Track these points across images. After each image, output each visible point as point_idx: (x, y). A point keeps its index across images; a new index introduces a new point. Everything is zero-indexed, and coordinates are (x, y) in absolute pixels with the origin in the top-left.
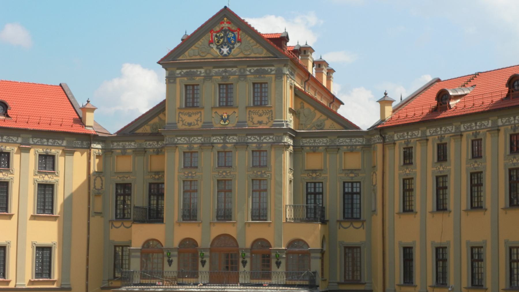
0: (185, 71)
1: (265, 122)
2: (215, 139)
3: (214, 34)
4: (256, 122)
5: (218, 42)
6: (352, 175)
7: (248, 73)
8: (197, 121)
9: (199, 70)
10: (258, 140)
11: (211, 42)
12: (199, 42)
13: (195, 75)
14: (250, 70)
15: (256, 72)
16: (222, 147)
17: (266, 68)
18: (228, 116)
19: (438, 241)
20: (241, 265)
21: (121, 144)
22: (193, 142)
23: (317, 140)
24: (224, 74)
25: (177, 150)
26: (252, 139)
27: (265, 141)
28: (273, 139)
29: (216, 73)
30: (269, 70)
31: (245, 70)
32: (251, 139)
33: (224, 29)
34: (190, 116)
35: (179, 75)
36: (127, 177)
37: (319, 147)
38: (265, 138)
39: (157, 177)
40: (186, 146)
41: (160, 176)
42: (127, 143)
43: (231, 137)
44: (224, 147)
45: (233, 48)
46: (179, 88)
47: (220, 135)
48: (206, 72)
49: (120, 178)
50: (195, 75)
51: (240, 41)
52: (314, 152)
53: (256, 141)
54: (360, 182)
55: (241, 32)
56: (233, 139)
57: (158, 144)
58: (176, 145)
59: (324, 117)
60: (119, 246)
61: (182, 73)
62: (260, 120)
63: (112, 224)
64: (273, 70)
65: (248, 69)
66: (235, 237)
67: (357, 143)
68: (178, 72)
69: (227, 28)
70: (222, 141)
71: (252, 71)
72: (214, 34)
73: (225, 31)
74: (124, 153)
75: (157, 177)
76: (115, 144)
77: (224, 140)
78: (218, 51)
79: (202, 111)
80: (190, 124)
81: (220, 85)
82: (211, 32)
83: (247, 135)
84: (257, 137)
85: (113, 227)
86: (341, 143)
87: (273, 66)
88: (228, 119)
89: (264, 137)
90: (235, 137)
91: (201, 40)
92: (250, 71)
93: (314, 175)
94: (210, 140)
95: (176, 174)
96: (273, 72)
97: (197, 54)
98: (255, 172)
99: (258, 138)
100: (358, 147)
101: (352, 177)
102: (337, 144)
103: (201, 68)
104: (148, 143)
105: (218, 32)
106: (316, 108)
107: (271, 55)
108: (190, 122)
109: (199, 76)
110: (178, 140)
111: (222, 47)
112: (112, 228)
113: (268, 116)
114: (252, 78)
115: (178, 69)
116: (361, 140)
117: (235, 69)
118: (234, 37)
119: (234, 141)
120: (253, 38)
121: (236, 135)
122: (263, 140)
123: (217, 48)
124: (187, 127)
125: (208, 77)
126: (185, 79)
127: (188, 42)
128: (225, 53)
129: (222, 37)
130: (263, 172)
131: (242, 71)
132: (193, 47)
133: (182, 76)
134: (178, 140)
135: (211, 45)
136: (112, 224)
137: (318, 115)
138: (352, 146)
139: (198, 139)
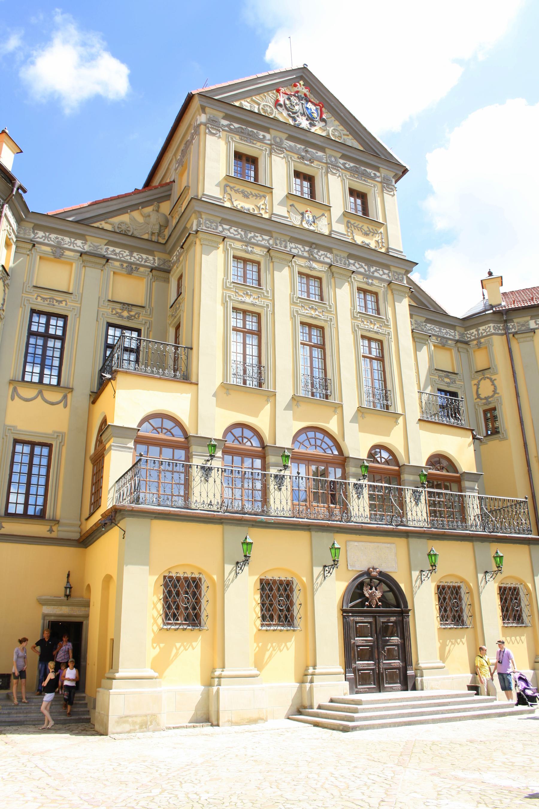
0: (237, 125)
9: (262, 133)
10: (365, 271)
14: (345, 164)
17: (369, 170)
21: (53, 236)
22: (253, 240)
24: (303, 154)
27: (376, 274)
28: (389, 277)
35: (226, 128)
36: (61, 302)
39: (125, 314)
41: (132, 313)
42: (67, 239)
43: (322, 252)
49: (44, 299)
53: (362, 270)
57: (131, 255)
60: (24, 443)
63: (15, 389)
64: (378, 177)
67: (448, 336)
68: (225, 122)
71: (347, 166)
74: (58, 253)
75: (125, 314)
76: (41, 234)
77: (310, 253)
84: (363, 264)
85: (16, 397)
86: (429, 330)
87: (377, 169)
89: (374, 268)
90: (329, 255)
92: (344, 164)
96: (379, 179)
99: (366, 268)
100: (450, 342)
103: (267, 130)
104: (111, 249)
110: (224, 229)
111: (298, 116)
112: (13, 399)
117: (320, 154)
119: (328, 261)
122: (373, 273)
134: (224, 229)
136: (15, 389)
139: (263, 239)
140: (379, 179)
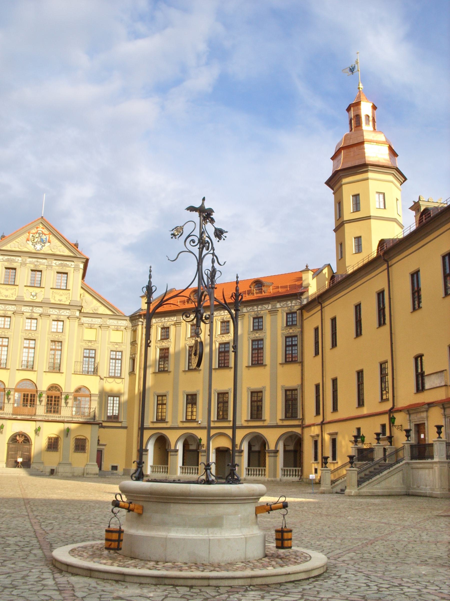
1: (64, 300)
2: (24, 309)
3: (32, 235)
5: (34, 241)
6: (117, 346)
7: (54, 265)
11: (28, 240)
12: (19, 239)
15: (61, 265)
16: (30, 315)
17: (68, 263)
18: (36, 294)
20: (38, 403)
22: (8, 309)
24: (36, 263)
26: (54, 311)
27: (63, 314)
29: (30, 262)
30: (70, 265)
31: (52, 263)
33: (39, 232)
34: (7, 290)
37: (94, 324)
38: (63, 312)
45: (44, 246)
48: (22, 260)
51: (49, 242)
53: (56, 313)
55: (51, 236)
56: (39, 310)
59: (99, 304)
61: (4, 259)
62: (60, 299)
65: (55, 262)
69: (41, 232)
70: (30, 311)
72: (32, 235)
73: (39, 234)
77: (32, 310)
80: (6, 296)
82: (29, 233)
88: (36, 295)
91: (21, 237)
92: (55, 264)
94: (21, 309)
97: (17, 247)
98: (54, 335)
99: (58, 312)
102: (108, 324)
105: (34, 234)
107: (72, 255)
108: (6, 295)
111: (36, 244)
113: (66, 297)
118: (46, 239)
119: (40, 312)
123: (32, 245)
124: (4, 298)
129: (37, 238)
130: (60, 336)
131: (50, 263)
132: (14, 242)
133: (4, 261)
135: (28, 242)
137: (95, 302)
138: (117, 326)
140: (73, 266)
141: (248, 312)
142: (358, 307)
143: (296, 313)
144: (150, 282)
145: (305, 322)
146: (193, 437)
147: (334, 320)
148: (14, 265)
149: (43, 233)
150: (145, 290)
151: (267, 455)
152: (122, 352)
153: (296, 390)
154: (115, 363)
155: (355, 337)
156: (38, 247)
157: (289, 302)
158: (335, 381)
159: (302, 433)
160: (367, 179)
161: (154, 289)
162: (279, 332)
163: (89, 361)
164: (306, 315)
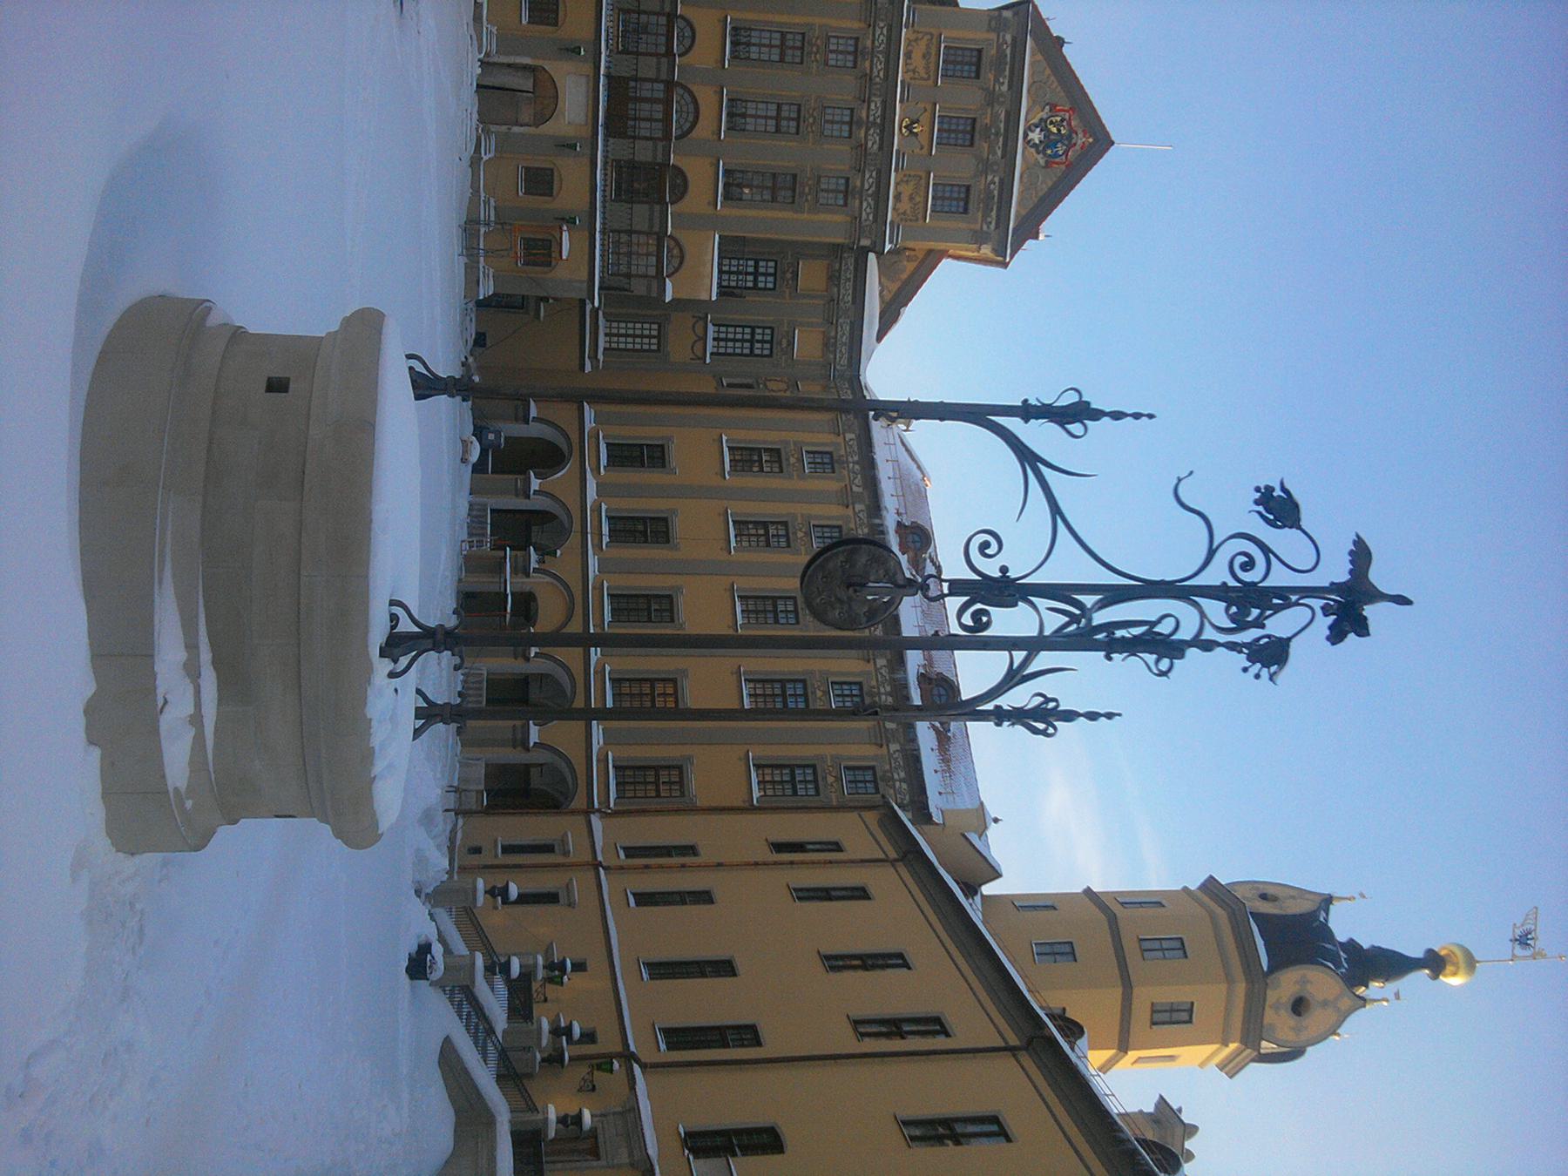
0: (1008, 52)
4: (900, 188)
6: (784, 342)
8: (914, 71)
11: (1053, 107)
13: (999, 72)
17: (994, 214)
19: (678, 527)
23: (849, 285)
25: (862, 25)
32: (870, 179)
37: (838, 286)
40: (869, 43)
44: (860, 123)
46: (979, 36)
47: (883, 117)
48: (1002, 95)
50: (999, 72)
51: (1048, 165)
52: (830, 278)
54: (770, 355)
56: (873, 145)
58: (872, 25)
66: (694, 134)
68: (1008, 38)
73: (1069, 137)
77: (874, 123)
78: (1036, 121)
79: (930, 82)
81: (974, 120)
83: (879, 172)
93: (789, 275)
95: (817, 21)
101: (780, 343)
103: (1010, 87)
105: (1069, 124)
106: (906, 283)
109: (996, 80)
114: (979, 186)
115: (1014, 39)
116: (844, 361)
118: (1056, 155)
120: (1051, 189)
121: (881, 148)
125: (991, 98)
126: (994, 52)
127: (1052, 46)
128: (1031, 135)
133: (999, 46)
138: (835, 344)
141: (877, 670)
142: (897, 960)
143: (877, 791)
144: (1097, 415)
145: (855, 815)
146: (563, 533)
147: (861, 893)
148: (989, 76)
149: (1071, 146)
150: (1070, 399)
151: (518, 723)
152: (770, 355)
153: (683, 795)
154: (743, 341)
155: (824, 951)
156: (1036, 136)
157: (902, 775)
158: (705, 897)
159: (573, 812)
160: (1230, 980)
161: (1076, 428)
162: (828, 751)
163: (747, 274)
164: (871, 817)
